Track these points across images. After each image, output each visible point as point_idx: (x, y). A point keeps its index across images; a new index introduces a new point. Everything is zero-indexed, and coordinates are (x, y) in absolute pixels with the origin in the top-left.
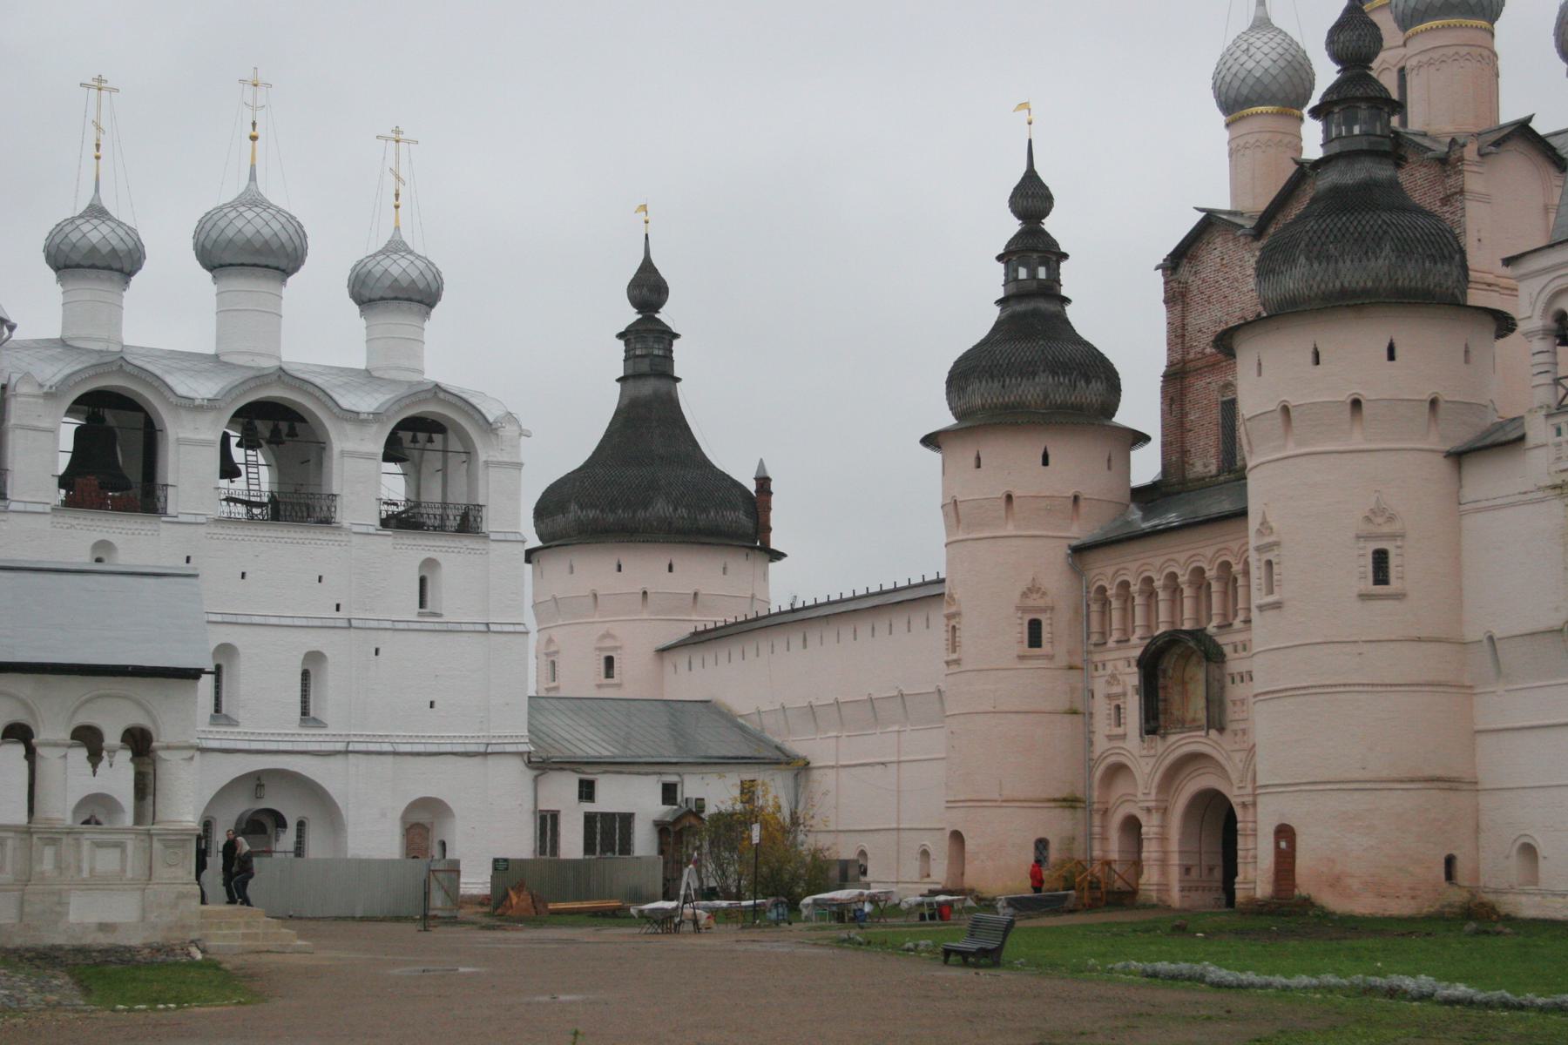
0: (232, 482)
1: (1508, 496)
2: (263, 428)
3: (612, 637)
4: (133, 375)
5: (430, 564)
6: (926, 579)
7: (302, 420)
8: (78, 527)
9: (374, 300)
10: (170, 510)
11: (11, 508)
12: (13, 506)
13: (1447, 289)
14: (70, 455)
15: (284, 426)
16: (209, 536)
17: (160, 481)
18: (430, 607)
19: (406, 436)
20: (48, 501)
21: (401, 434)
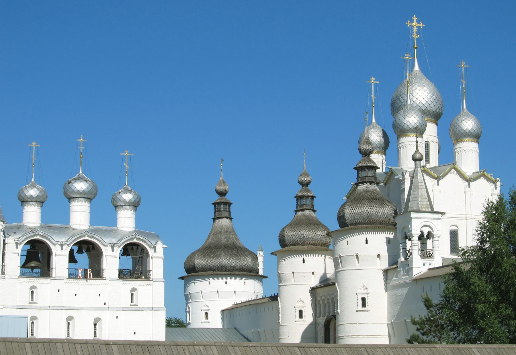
0: (75, 264)
1: (418, 273)
2: (85, 247)
3: (207, 306)
4: (42, 235)
5: (134, 289)
6: (266, 297)
7: (94, 244)
8: (26, 282)
9: (119, 206)
10: (54, 275)
11: (6, 277)
12: (7, 277)
13: (381, 221)
14: (26, 256)
15: (91, 246)
16: (65, 283)
17: (51, 267)
18: (134, 303)
19: (129, 248)
20: (17, 275)
21: (128, 247)
